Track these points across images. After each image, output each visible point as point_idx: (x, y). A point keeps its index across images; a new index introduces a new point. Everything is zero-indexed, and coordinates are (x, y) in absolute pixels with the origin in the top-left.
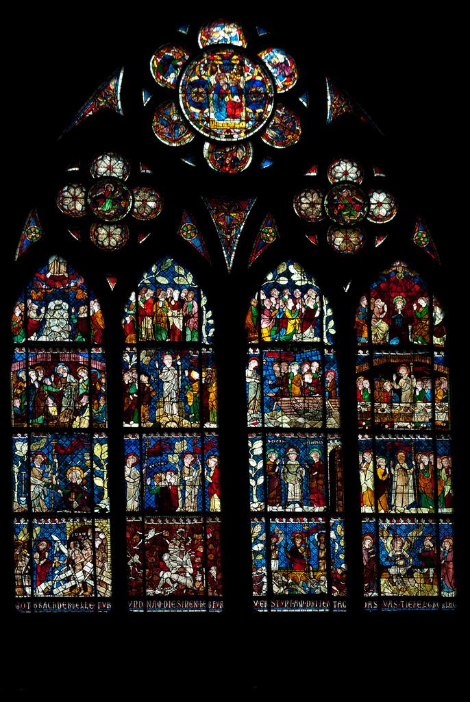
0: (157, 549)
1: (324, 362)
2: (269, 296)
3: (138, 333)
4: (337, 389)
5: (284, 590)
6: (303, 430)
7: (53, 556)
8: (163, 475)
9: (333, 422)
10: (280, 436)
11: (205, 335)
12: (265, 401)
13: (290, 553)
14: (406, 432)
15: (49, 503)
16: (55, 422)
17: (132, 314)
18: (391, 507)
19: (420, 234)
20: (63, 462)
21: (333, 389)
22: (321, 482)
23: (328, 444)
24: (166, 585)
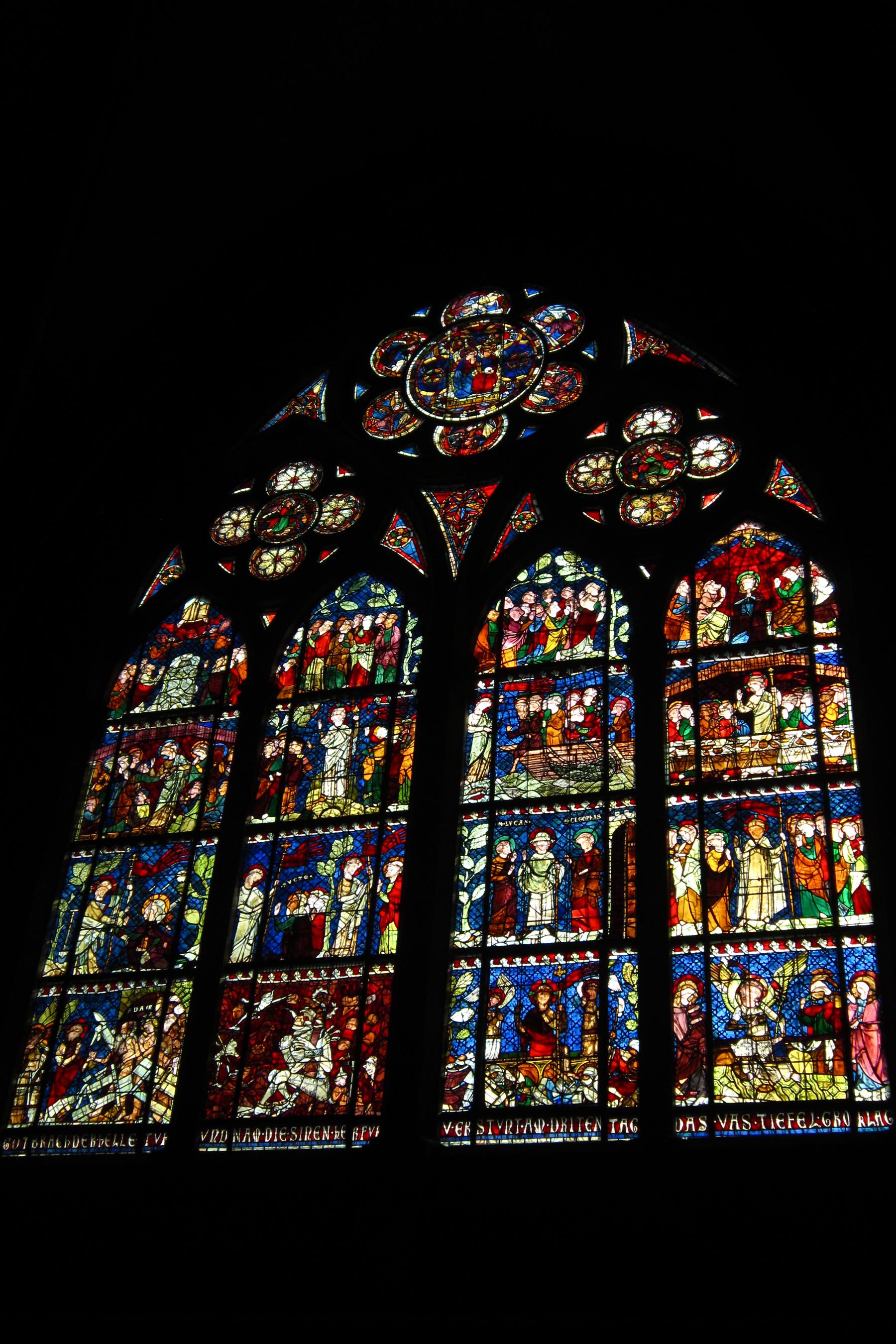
2: (518, 603)
4: (632, 727)
5: (508, 1098)
6: (565, 799)
9: (622, 780)
10: (522, 813)
11: (407, 672)
18: (735, 920)
21: (623, 727)
22: (593, 886)
23: (611, 818)
24: (277, 1097)
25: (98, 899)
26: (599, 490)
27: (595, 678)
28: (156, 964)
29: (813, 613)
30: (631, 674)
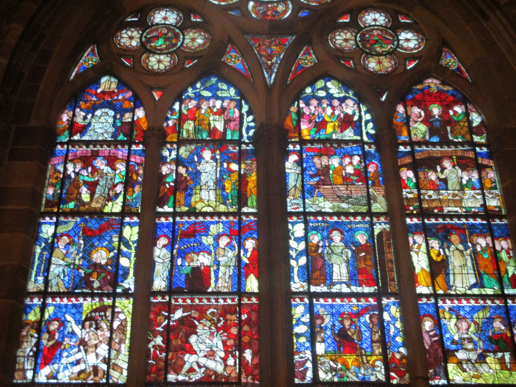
0: (184, 330)
1: (365, 156)
3: (179, 133)
5: (333, 376)
7: (63, 338)
8: (195, 256)
12: (306, 188)
13: (338, 335)
14: (459, 217)
15: (68, 282)
16: (87, 207)
17: (175, 119)
18: (450, 287)
19: (448, 60)
20: (89, 243)
21: (376, 179)
25: (61, 247)
26: (349, 50)
27: (358, 150)
28: (104, 289)
29: (472, 130)
30: (377, 150)
